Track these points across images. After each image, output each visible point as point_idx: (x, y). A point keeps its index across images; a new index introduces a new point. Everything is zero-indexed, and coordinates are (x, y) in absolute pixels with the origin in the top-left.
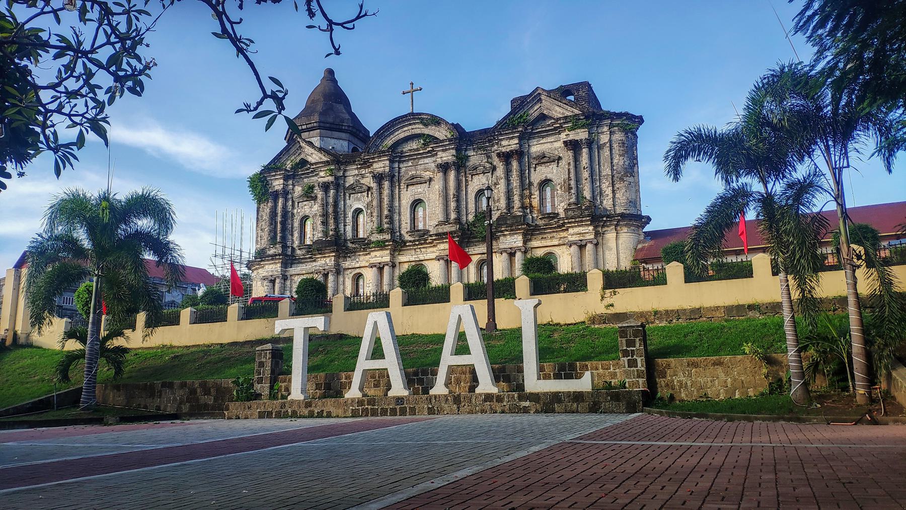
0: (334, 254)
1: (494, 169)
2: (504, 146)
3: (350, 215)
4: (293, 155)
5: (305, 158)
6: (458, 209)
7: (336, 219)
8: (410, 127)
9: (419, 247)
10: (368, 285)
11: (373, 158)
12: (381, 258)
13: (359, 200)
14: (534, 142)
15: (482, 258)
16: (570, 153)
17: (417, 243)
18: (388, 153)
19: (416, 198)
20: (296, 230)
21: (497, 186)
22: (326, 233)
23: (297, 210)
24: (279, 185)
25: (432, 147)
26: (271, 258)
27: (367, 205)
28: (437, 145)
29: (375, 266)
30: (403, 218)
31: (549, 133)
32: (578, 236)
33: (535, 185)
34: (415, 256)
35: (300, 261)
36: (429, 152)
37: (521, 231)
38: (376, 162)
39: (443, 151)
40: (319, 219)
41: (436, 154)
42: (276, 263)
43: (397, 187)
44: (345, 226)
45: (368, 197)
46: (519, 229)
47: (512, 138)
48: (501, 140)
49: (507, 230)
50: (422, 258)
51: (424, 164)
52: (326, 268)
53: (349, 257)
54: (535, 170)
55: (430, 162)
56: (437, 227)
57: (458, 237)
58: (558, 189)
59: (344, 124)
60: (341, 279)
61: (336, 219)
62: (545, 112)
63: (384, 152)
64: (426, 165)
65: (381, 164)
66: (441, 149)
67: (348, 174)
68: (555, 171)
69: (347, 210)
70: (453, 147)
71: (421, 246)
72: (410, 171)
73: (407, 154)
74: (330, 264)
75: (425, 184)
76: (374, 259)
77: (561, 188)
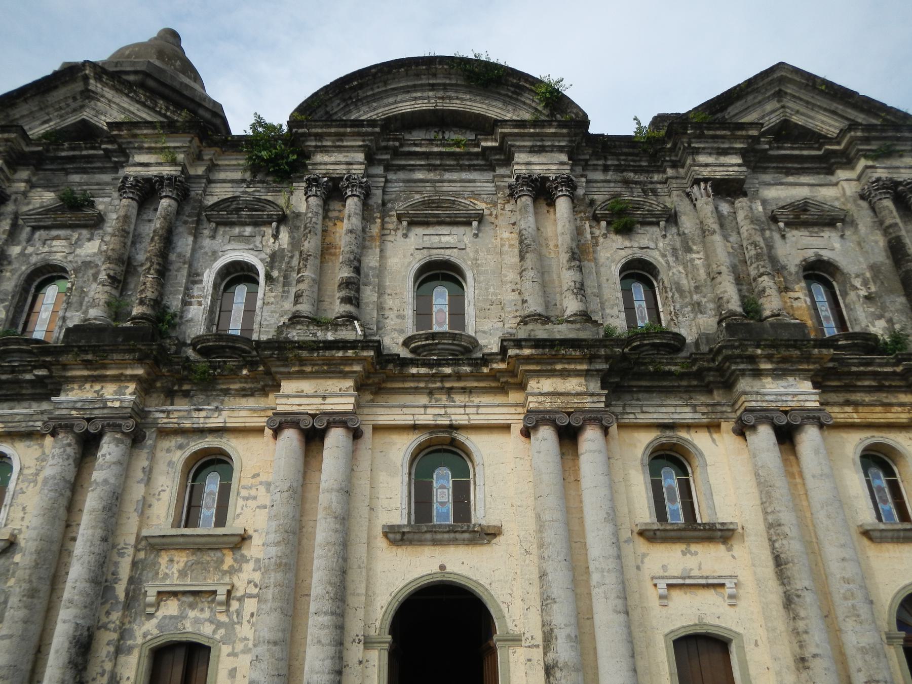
0: (140, 372)
1: (672, 218)
2: (707, 165)
3: (209, 277)
4: (57, 110)
6: (580, 289)
7: (163, 273)
8: (431, 93)
9: (448, 385)
11: (319, 137)
12: (319, 400)
13: (247, 239)
14: (767, 178)
15: (664, 440)
16: (888, 203)
17: (448, 370)
18: (369, 130)
19: (434, 258)
21: (689, 256)
22: (116, 310)
23: (25, 248)
25: (504, 136)
27: (273, 256)
28: (522, 131)
29: (295, 424)
30: (389, 302)
31: (806, 165)
33: (793, 269)
34: (437, 411)
36: (485, 149)
37: (811, 367)
38: (324, 150)
39: (532, 150)
40: (103, 267)
41: (508, 161)
43: (379, 221)
44: (186, 303)
45: (276, 236)
46: (807, 358)
48: (697, 151)
49: (769, 358)
51: (462, 181)
53: (186, 394)
54: (783, 237)
55: (482, 182)
56: (530, 326)
57: (607, 358)
58: (859, 286)
59: (204, 104)
60: (142, 461)
61: (163, 273)
62: (795, 119)
63: (358, 123)
64: (467, 184)
65: (341, 157)
67: (222, 175)
68: (837, 245)
69: (198, 265)
71: (456, 385)
72: (417, 192)
73: (418, 149)
74: (117, 404)
75: (461, 230)
76: (292, 401)
77: (865, 283)
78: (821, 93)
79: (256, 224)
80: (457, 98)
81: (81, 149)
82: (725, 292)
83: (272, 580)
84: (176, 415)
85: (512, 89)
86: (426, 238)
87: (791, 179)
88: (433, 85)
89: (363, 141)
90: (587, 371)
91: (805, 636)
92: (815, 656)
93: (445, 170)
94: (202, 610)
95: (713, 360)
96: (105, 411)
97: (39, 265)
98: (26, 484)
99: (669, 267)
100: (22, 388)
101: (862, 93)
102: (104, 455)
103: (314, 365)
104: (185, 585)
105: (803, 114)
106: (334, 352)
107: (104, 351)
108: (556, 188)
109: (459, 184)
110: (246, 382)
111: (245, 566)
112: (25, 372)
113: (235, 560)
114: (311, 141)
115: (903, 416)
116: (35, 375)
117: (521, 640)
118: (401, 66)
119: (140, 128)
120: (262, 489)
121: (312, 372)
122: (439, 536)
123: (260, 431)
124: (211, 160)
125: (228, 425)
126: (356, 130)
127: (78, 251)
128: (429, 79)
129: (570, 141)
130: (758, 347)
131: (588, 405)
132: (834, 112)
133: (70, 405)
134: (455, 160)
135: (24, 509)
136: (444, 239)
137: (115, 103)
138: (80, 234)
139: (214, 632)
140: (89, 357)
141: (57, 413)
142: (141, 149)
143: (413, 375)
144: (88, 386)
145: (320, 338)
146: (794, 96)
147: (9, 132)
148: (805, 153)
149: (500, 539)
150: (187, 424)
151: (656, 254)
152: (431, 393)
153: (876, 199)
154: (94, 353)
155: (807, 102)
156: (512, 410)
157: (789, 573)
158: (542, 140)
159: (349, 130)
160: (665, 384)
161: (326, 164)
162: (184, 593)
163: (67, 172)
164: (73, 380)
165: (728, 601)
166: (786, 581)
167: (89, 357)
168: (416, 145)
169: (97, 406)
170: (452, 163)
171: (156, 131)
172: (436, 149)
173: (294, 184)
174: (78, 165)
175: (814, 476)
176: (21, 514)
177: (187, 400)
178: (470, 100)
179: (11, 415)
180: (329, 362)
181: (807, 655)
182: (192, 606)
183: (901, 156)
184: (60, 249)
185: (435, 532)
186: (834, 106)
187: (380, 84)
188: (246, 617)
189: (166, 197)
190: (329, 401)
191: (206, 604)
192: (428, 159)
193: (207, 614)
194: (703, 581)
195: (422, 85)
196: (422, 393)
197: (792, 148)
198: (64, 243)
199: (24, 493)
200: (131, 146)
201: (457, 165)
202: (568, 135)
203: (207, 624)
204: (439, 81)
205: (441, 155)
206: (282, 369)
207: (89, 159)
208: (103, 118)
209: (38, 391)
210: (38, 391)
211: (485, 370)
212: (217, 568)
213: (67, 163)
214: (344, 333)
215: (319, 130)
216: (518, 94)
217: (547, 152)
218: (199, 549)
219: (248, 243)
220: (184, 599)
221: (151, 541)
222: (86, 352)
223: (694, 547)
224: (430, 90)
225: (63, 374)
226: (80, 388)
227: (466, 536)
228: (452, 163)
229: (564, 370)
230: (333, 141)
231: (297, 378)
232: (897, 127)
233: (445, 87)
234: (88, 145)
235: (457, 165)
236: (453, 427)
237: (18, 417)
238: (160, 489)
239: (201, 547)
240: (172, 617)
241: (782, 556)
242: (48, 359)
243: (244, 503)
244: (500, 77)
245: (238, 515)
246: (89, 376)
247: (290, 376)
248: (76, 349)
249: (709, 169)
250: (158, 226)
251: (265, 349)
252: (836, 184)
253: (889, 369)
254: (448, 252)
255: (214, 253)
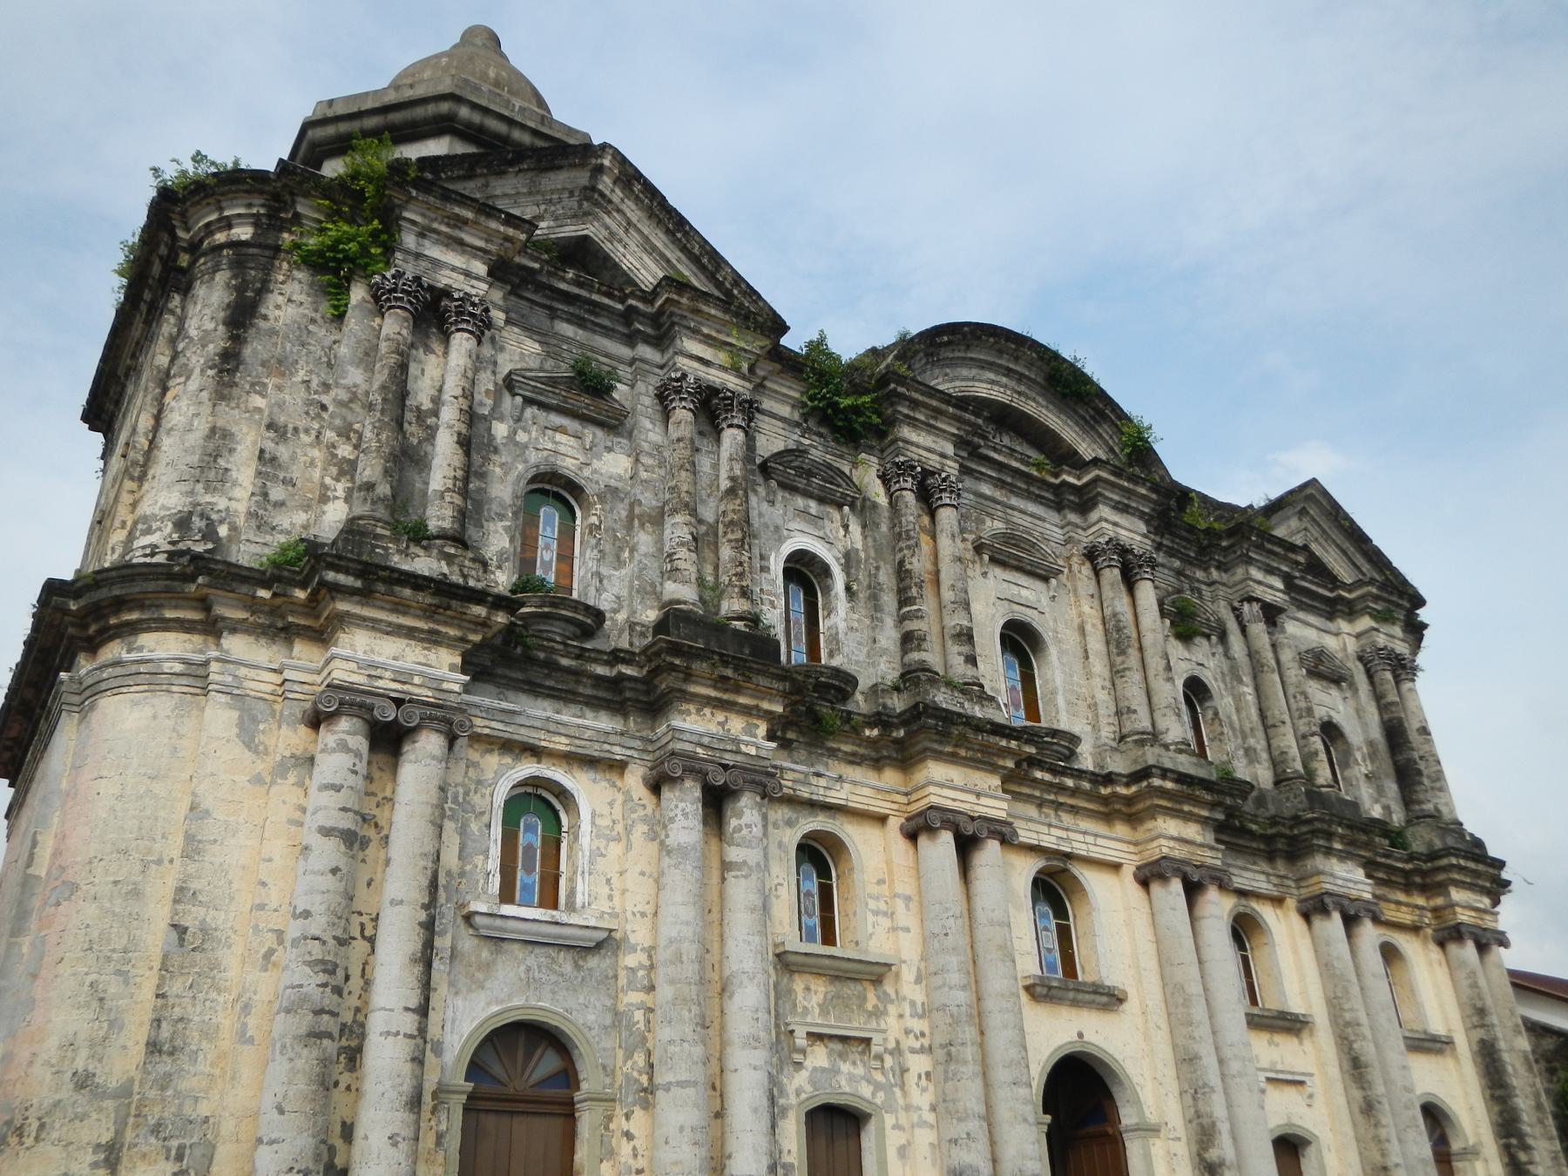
0: (779, 709)
3: (777, 565)
5: (607, 247)
8: (1004, 380)
9: (1061, 799)
10: (872, 904)
11: (915, 404)
12: (972, 798)
17: (1070, 783)
18: (972, 418)
20: (502, 517)
24: (467, 274)
26: (426, 599)
32: (1473, 914)
35: (537, 675)
36: (1064, 483)
38: (913, 422)
42: (433, 639)
47: (1270, 571)
48: (1249, 561)
49: (1342, 837)
50: (1080, 848)
51: (1031, 515)
52: (729, 759)
66: (1116, 498)
68: (1341, 708)
70: (1147, 510)
72: (989, 514)
73: (996, 456)
74: (753, 751)
75: (1039, 585)
78: (1341, 527)
79: (821, 500)
80: (1034, 400)
81: (590, 289)
82: (1290, 747)
83: (968, 1036)
84: (790, 775)
85: (1092, 412)
86: (1005, 584)
87: (1301, 615)
88: (1009, 370)
89: (958, 429)
90: (1207, 818)
91: (1387, 1145)
92: (1397, 1165)
93: (1012, 492)
94: (854, 1063)
95: (1291, 828)
96: (739, 758)
97: (543, 469)
98: (604, 842)
99: (1222, 697)
100: (578, 682)
101: (1375, 542)
102: (748, 826)
103: (968, 749)
104: (827, 1026)
105: (1320, 544)
106: (998, 738)
107: (750, 669)
108: (1140, 566)
109: (1029, 519)
110: (859, 745)
111: (892, 1009)
112: (595, 661)
113: (878, 998)
114: (903, 406)
115: (1408, 917)
116: (620, 673)
117: (1159, 1131)
118: (992, 335)
119: (707, 303)
120: (900, 905)
121: (965, 758)
122: (1080, 996)
123: (882, 819)
124: (765, 378)
125: (850, 804)
126: (959, 413)
127: (596, 464)
128: (1009, 361)
129: (1153, 510)
130: (1340, 825)
131: (1209, 861)
132: (1344, 552)
133: (695, 738)
134: (1027, 483)
135: (608, 881)
136: (1024, 592)
137: (639, 231)
138: (594, 434)
139: (873, 1094)
140: (729, 673)
141: (679, 746)
142: (695, 332)
143: (1035, 780)
144: (707, 711)
145: (969, 712)
146: (1314, 520)
147: (516, 227)
148: (1320, 591)
149: (1126, 1006)
150: (805, 792)
151: (1209, 674)
152: (1041, 804)
153: (1379, 668)
154: (736, 669)
155: (1324, 531)
156: (1124, 847)
157: (1369, 1077)
158: (1129, 498)
159: (951, 410)
160: (1241, 842)
161: (918, 446)
162: (831, 1037)
163: (553, 314)
164: (693, 698)
165: (1309, 1101)
166: (1366, 1085)
167: (729, 673)
168: (995, 450)
169: (728, 747)
170: (1023, 486)
171: (727, 318)
172: (1015, 464)
173: (863, 455)
174: (577, 312)
175: (1373, 975)
176: (606, 890)
177: (786, 753)
178: (1047, 408)
179: (579, 726)
180: (985, 749)
181: (1389, 1164)
182: (842, 1056)
183: (1394, 624)
184: (571, 452)
185: (1078, 991)
186: (1347, 545)
187: (963, 348)
188: (911, 1078)
189: (739, 427)
190: (984, 801)
191: (858, 1056)
192: (999, 471)
193: (860, 1070)
194: (1290, 1077)
195: (1000, 366)
196: (1032, 803)
197: (1312, 582)
198: (572, 441)
199: (603, 855)
200: (685, 323)
201: (1027, 491)
202: (1155, 502)
203: (864, 1084)
204: (1018, 368)
205: (1016, 471)
206: (936, 746)
207: (596, 307)
208: (622, 250)
209: (601, 694)
210: (601, 694)
211: (1104, 791)
212: (861, 1006)
213: (558, 300)
214: (991, 711)
215: (920, 398)
216: (1097, 422)
217: (1128, 513)
218: (837, 977)
219: (816, 526)
220: (832, 1045)
221: (791, 958)
222: (725, 664)
223: (1278, 1038)
224: (1004, 375)
225: (684, 687)
226: (699, 711)
227: (1104, 999)
228: (1023, 486)
229: (1190, 813)
230: (926, 416)
231: (946, 761)
232: (1401, 594)
233: (1021, 378)
234: (604, 288)
235: (1027, 491)
236: (1068, 856)
237: (588, 734)
238: (776, 882)
239: (840, 974)
240: (823, 1070)
241: (1362, 1058)
242: (677, 662)
243: (875, 919)
244: (1088, 394)
245: (871, 935)
246: (716, 699)
247: (940, 756)
248: (716, 657)
249: (1262, 588)
250: (738, 473)
251: (931, 716)
252: (1337, 634)
253: (1400, 865)
254: (1029, 612)
255: (777, 528)
